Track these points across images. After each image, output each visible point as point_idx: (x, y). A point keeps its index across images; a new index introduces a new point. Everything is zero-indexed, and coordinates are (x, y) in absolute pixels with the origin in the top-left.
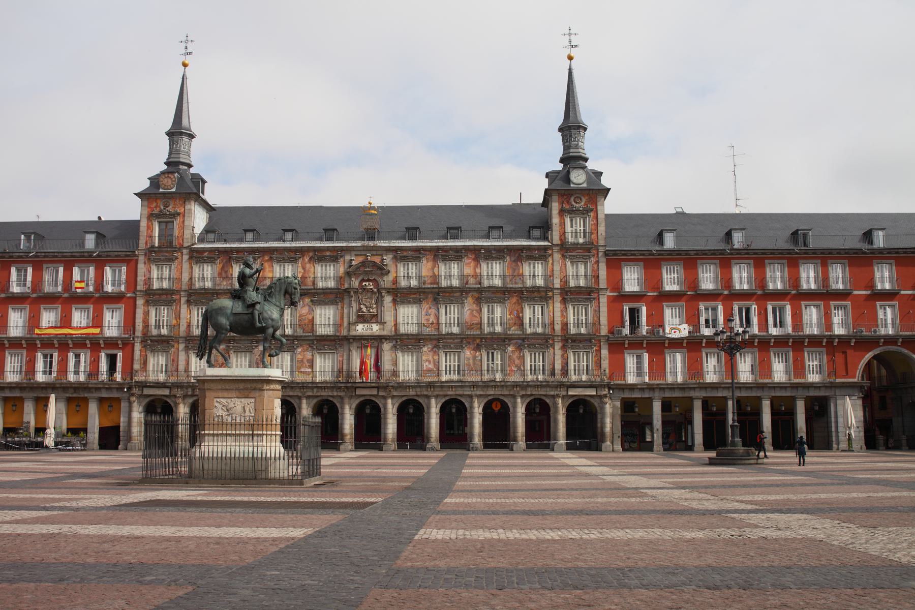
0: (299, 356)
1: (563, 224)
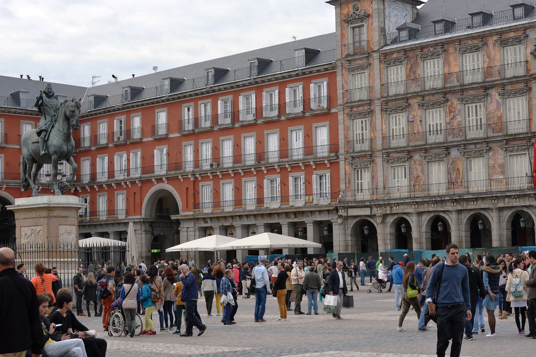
0: (491, 162)
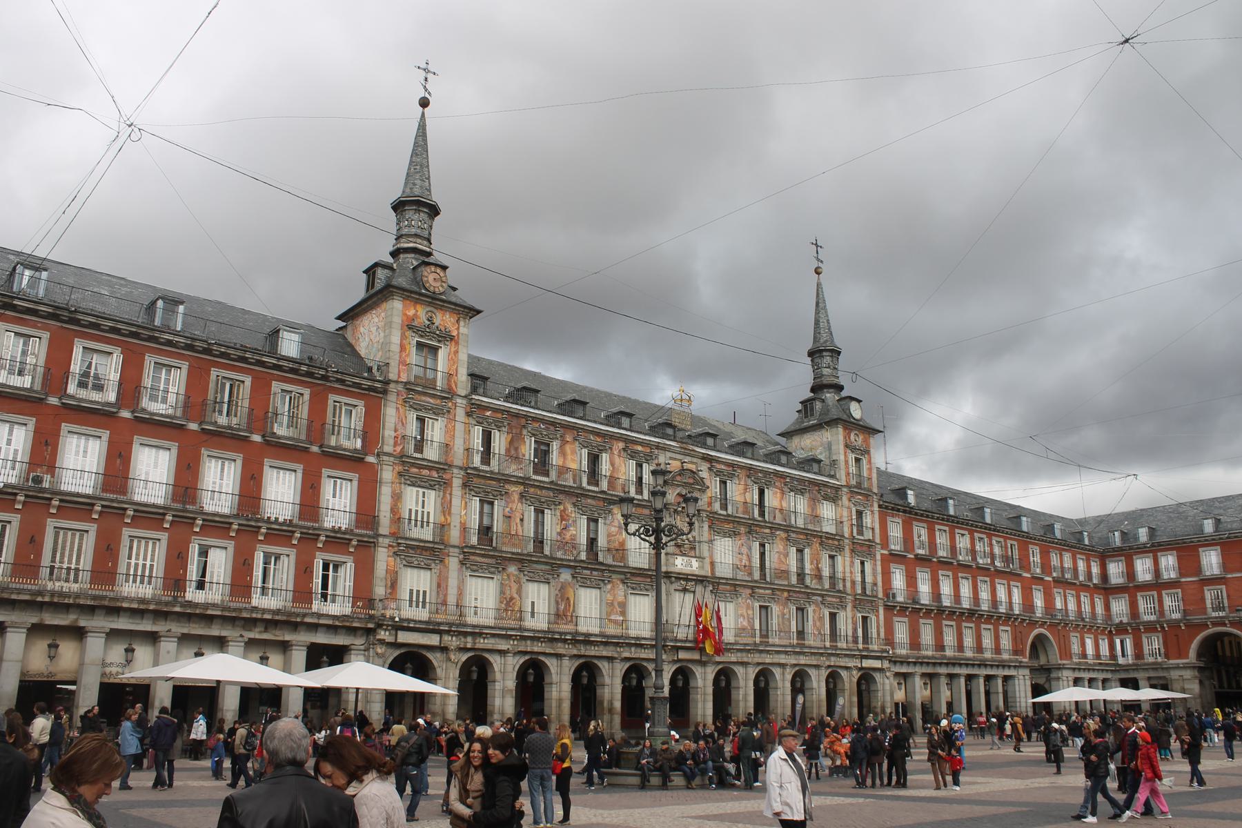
0: (610, 597)
1: (846, 462)
